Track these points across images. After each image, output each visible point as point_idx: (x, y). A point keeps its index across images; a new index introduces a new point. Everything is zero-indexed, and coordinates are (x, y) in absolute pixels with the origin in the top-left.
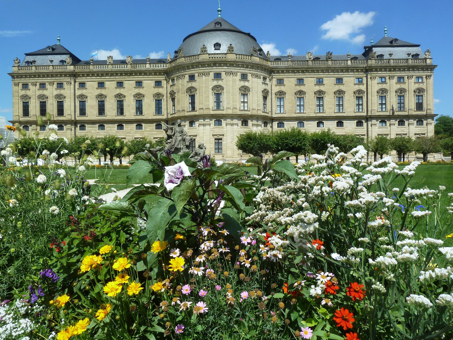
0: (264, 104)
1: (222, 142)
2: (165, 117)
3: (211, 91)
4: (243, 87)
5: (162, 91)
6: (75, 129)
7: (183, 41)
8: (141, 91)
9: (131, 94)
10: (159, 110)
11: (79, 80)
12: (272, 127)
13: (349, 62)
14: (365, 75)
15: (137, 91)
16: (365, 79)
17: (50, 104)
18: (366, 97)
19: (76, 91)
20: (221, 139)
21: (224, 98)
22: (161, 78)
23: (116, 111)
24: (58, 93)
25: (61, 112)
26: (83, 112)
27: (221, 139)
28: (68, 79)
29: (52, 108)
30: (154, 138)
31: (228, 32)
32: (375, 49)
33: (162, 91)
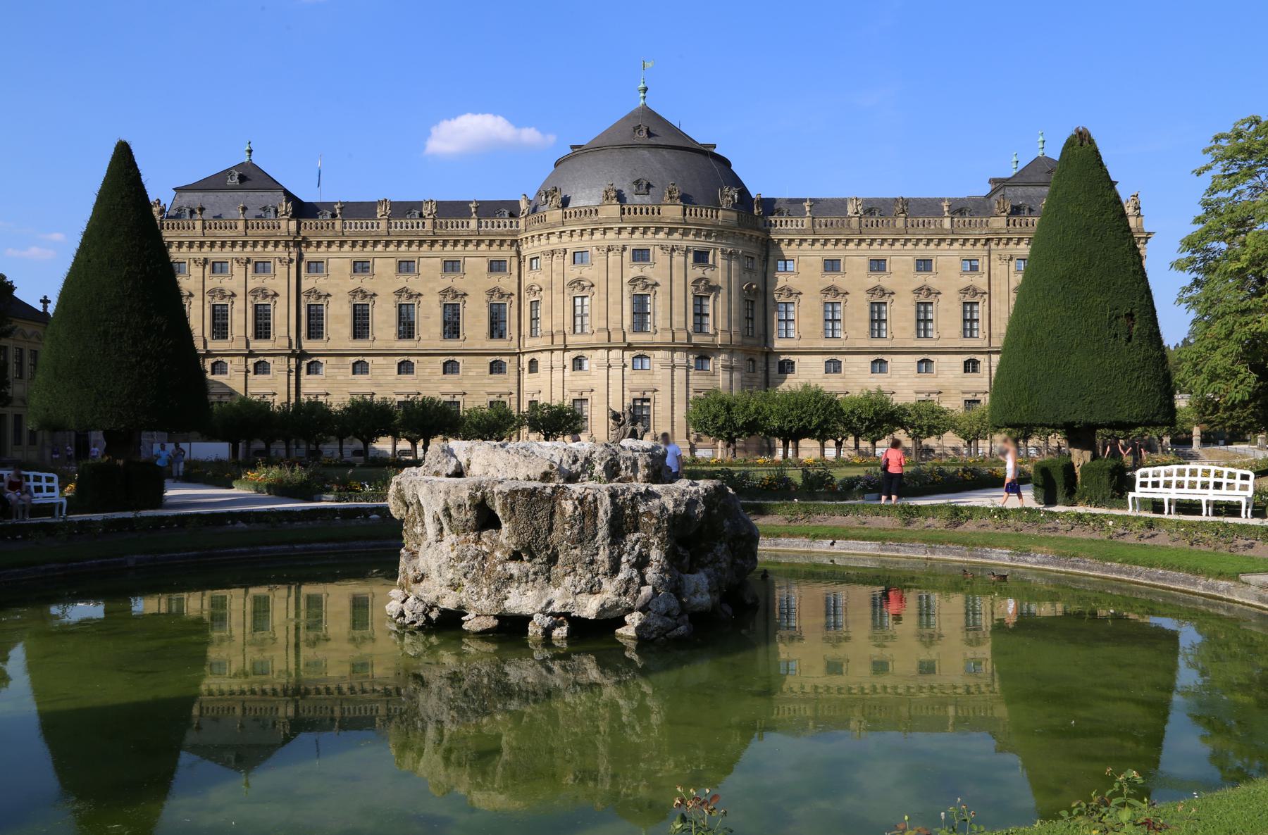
0: (747, 318)
1: (649, 407)
2: (513, 345)
3: (627, 288)
4: (699, 280)
5: (507, 283)
6: (298, 368)
7: (556, 165)
8: (458, 283)
9: (433, 289)
10: (496, 327)
11: (310, 254)
12: (767, 372)
13: (947, 223)
14: (986, 253)
15: (447, 281)
16: (986, 259)
17: (239, 311)
18: (987, 303)
19: (303, 281)
20: (648, 400)
21: (658, 306)
22: (506, 253)
23: (393, 331)
24: (257, 285)
25: (262, 329)
26: (316, 330)
27: (648, 400)
28: (281, 252)
29: (240, 321)
30: (489, 394)
31: (665, 152)
32: (1009, 192)
33: (507, 283)
